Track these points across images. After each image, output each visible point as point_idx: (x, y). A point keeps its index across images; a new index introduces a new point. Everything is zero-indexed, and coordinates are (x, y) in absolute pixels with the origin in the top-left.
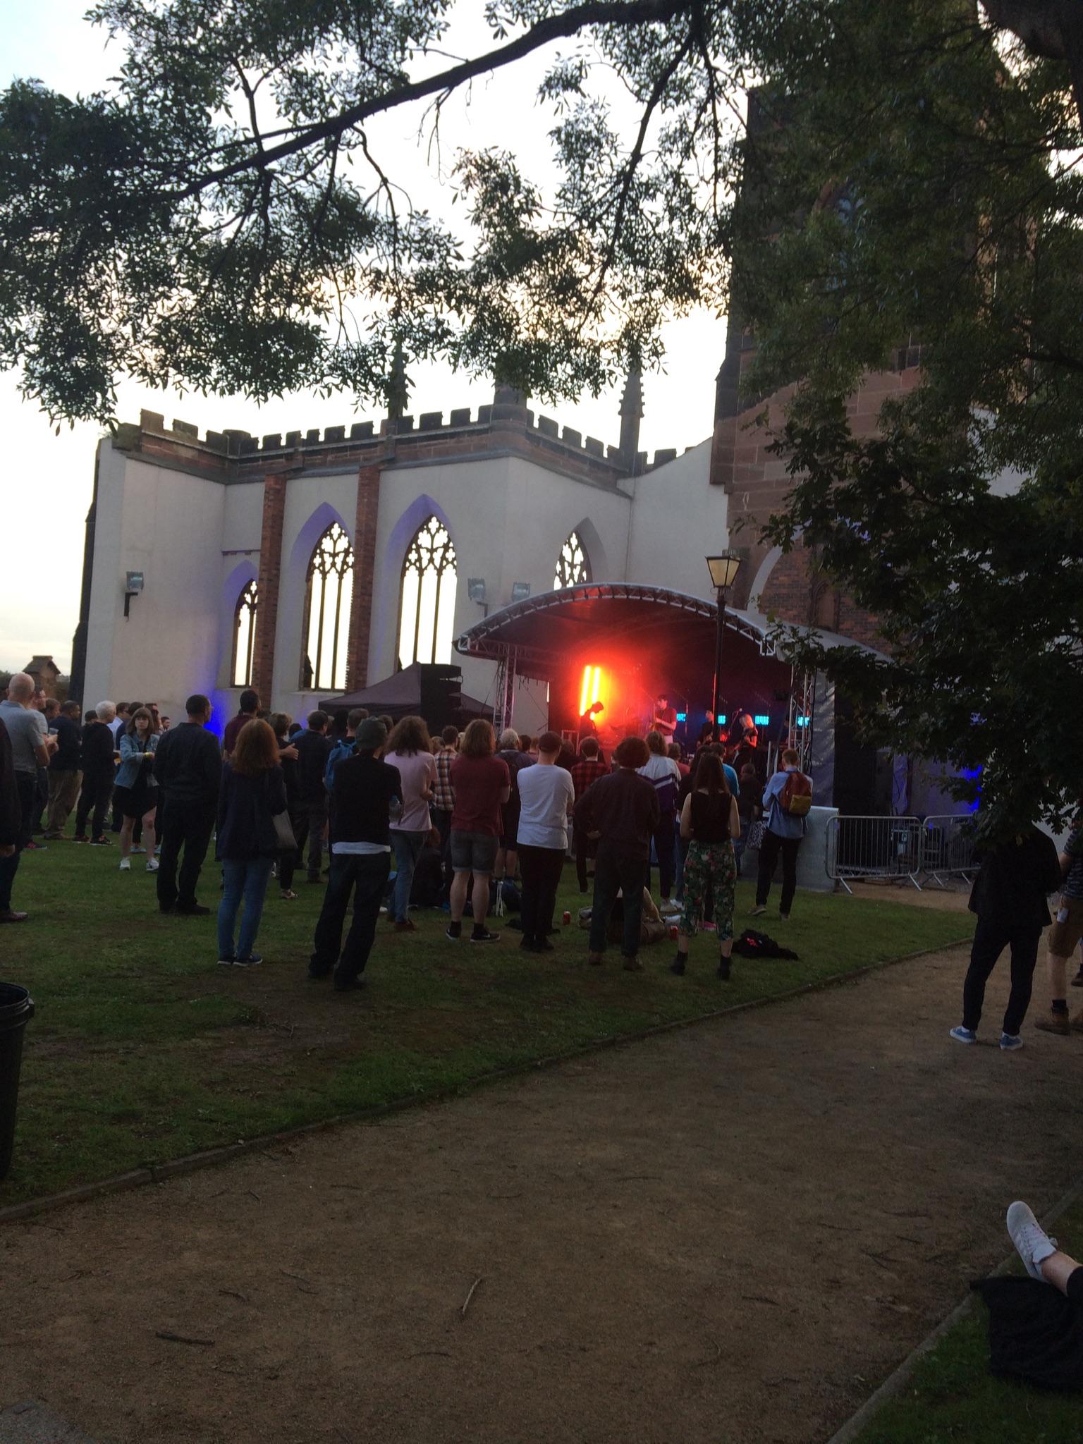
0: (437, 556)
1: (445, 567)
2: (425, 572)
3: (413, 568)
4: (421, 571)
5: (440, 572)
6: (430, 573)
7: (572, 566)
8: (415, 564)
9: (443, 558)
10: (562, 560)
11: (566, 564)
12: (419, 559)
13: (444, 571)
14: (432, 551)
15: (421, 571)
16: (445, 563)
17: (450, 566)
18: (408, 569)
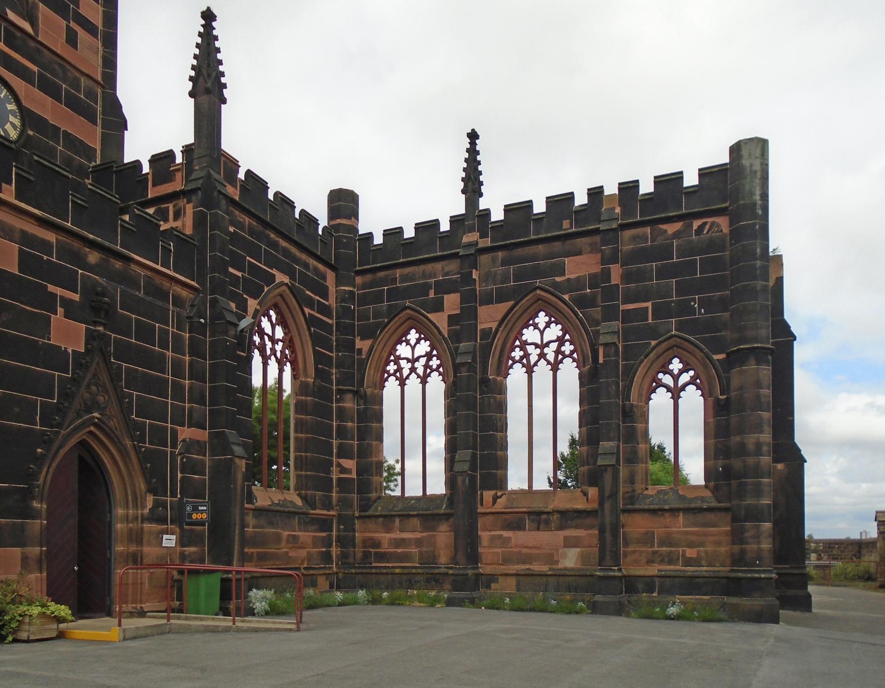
0: (420, 366)
1: (429, 375)
2: (407, 381)
3: (392, 379)
4: (402, 383)
5: (424, 381)
6: (413, 383)
7: (272, 339)
8: (394, 374)
9: (426, 366)
10: (262, 333)
11: (266, 338)
12: (400, 369)
13: (429, 379)
14: (413, 361)
15: (402, 383)
16: (429, 371)
17: (435, 374)
18: (386, 380)
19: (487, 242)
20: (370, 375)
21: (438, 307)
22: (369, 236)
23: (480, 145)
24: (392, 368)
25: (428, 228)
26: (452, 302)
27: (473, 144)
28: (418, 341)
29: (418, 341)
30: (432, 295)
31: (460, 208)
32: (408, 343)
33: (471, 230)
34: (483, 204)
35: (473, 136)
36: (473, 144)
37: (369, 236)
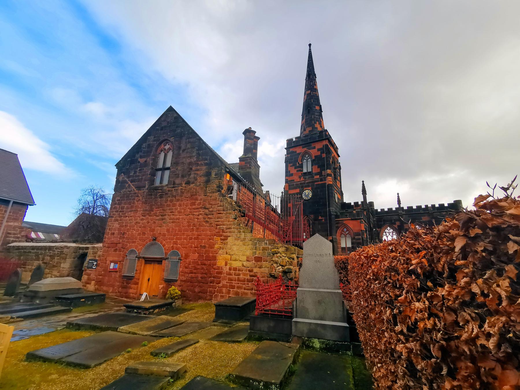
9: (392, 234)
19: (404, 213)
20: (380, 235)
21: (395, 224)
22: (377, 210)
23: (399, 195)
24: (384, 234)
25: (390, 210)
26: (398, 223)
27: (398, 195)
28: (390, 229)
29: (390, 229)
30: (393, 221)
31: (398, 206)
32: (388, 229)
33: (400, 210)
34: (401, 206)
35: (398, 194)
36: (398, 195)
37: (377, 210)
